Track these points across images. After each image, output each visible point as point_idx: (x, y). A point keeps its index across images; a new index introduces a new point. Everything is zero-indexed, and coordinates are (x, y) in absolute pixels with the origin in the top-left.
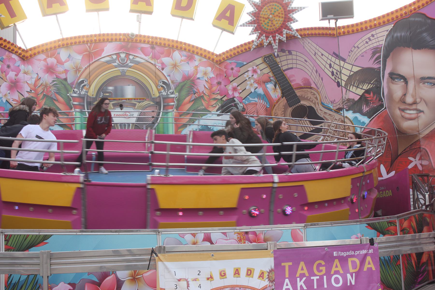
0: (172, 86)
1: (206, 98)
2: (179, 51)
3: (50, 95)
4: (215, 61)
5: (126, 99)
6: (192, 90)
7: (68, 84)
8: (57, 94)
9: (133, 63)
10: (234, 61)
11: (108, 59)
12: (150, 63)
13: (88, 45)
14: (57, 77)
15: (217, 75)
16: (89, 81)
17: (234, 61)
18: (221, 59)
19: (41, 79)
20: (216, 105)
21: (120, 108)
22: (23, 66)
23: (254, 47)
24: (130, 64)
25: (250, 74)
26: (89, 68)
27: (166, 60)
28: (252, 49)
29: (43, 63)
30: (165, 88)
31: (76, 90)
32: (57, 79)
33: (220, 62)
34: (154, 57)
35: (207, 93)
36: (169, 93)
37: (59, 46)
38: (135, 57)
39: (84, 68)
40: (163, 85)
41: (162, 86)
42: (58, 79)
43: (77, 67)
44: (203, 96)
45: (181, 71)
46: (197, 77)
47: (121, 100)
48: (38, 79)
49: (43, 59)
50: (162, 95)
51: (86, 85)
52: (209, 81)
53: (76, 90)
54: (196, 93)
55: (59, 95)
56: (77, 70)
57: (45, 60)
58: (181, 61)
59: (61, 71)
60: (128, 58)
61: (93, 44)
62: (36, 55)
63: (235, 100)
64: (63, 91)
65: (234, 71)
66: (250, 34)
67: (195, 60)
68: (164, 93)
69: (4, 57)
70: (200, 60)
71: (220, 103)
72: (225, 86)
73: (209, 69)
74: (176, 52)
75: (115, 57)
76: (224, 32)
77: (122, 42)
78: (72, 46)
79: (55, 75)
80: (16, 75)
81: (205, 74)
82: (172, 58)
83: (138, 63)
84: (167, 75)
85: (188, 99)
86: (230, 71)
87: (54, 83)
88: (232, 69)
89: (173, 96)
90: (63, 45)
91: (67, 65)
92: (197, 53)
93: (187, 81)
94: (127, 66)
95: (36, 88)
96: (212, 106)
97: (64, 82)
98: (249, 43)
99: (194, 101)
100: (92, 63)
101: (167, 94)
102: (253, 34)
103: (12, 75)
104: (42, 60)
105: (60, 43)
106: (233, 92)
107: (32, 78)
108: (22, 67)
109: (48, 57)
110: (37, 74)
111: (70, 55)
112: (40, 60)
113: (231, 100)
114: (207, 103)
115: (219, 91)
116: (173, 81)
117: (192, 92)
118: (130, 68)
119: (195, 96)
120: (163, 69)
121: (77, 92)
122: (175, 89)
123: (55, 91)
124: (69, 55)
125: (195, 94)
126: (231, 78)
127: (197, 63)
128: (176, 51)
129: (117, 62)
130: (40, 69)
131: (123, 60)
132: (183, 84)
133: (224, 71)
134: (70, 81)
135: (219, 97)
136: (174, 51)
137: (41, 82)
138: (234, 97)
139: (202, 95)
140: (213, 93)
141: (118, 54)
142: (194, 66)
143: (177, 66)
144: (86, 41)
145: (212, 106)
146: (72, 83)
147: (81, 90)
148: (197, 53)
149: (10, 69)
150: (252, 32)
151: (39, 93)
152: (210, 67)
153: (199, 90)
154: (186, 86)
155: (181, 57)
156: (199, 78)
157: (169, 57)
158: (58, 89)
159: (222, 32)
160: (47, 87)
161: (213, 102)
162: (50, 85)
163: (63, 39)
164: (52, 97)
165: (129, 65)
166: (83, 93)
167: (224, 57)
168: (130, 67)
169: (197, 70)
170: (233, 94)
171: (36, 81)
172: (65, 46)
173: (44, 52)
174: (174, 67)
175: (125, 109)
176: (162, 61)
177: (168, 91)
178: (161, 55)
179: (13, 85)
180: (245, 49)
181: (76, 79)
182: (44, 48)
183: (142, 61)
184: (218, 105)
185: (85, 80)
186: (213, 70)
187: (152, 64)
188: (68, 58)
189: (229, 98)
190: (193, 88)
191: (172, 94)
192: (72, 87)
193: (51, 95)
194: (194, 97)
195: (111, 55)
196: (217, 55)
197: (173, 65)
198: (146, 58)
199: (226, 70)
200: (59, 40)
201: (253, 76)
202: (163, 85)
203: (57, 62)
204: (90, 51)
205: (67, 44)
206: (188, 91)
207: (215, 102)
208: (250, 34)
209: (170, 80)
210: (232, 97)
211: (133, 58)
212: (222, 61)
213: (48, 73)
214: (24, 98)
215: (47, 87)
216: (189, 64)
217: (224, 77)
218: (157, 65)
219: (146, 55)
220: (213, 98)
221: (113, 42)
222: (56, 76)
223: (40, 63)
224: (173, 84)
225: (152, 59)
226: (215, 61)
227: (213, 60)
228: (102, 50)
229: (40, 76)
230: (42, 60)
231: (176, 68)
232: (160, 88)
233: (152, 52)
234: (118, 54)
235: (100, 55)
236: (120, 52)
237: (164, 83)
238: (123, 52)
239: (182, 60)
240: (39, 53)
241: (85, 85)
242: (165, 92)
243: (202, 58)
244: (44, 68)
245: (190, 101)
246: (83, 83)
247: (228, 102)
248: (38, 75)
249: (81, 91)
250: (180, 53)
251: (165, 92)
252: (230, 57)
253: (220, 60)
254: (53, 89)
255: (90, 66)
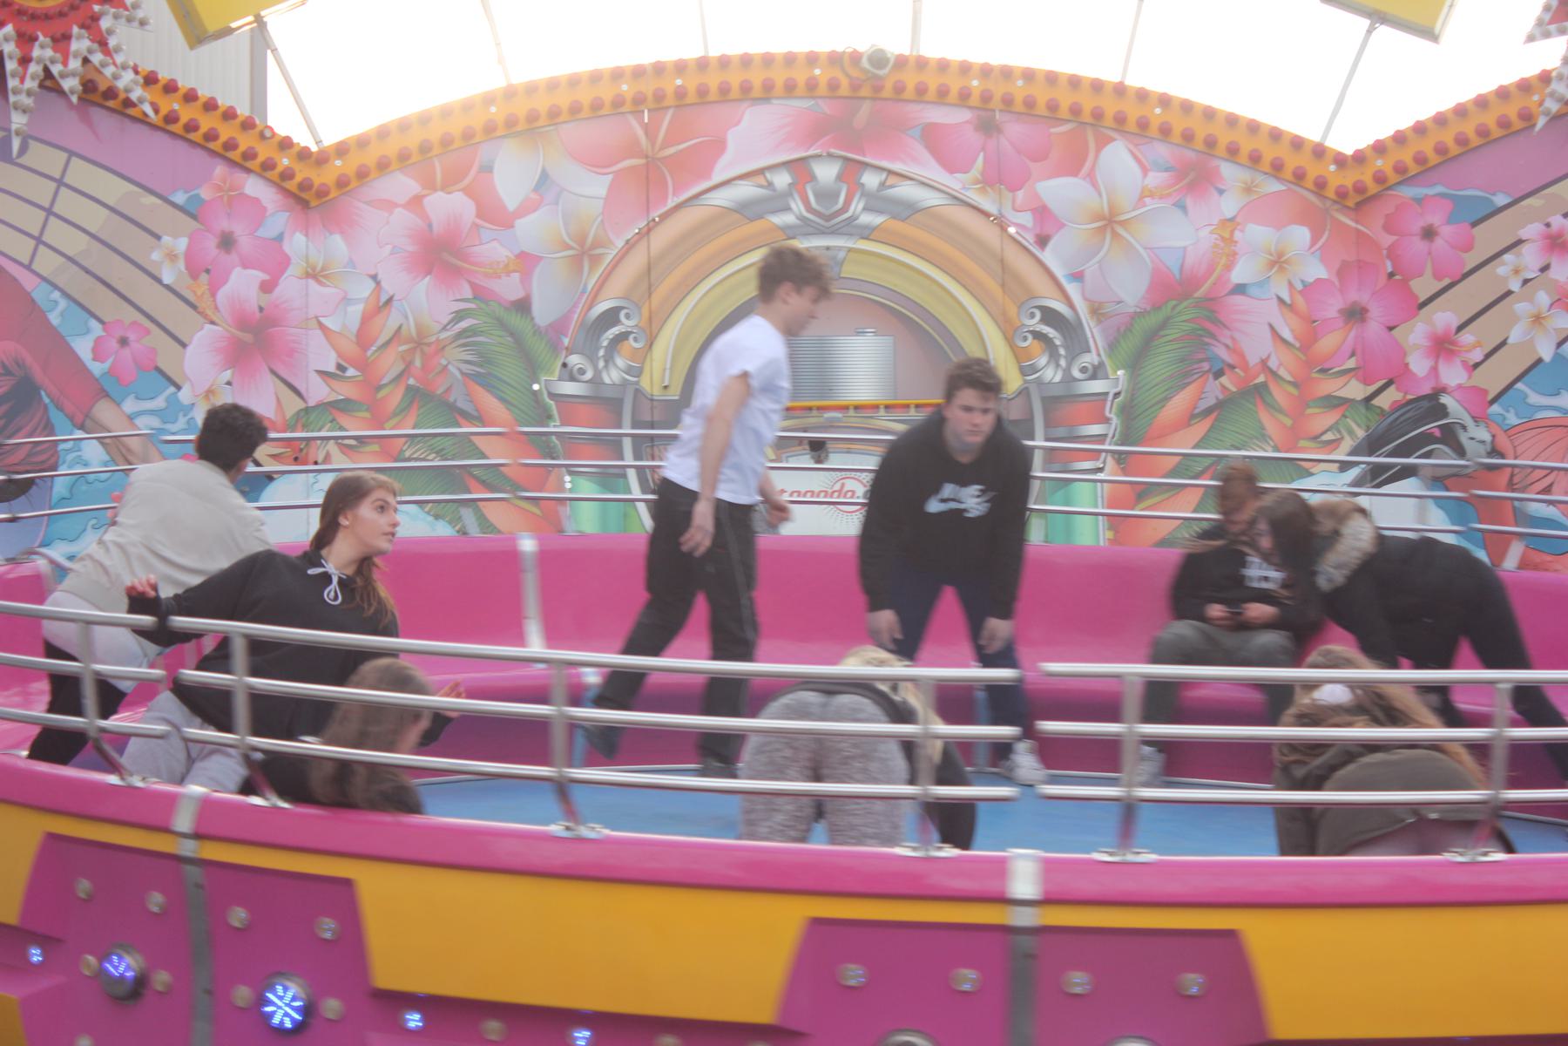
0: (1094, 333)
1: (1279, 395)
2: (1136, 145)
3: (439, 392)
4: (1330, 192)
5: (844, 408)
6: (1201, 356)
7: (537, 331)
8: (480, 385)
9: (881, 212)
10: (1439, 189)
11: (745, 191)
12: (971, 209)
13: (641, 121)
14: (480, 294)
15: (1343, 272)
16: (645, 311)
17: (1439, 189)
18: (1367, 178)
19: (395, 303)
20: (1339, 432)
21: (813, 457)
22: (299, 238)
23: (1553, 106)
24: (867, 219)
25: (1530, 257)
26: (644, 243)
27: (1058, 190)
28: (1541, 122)
29: (402, 219)
30: (1058, 342)
31: (575, 360)
32: (478, 302)
33: (1358, 200)
34: (995, 178)
35: (1290, 372)
36: (1076, 373)
37: (490, 129)
38: (890, 181)
39: (620, 244)
40: (1046, 329)
41: (1038, 336)
42: (483, 306)
43: (582, 242)
44: (1264, 385)
45: (1145, 248)
46: (1229, 280)
47: (815, 413)
48: (380, 308)
49: (402, 200)
50: (1039, 382)
51: (631, 332)
52: (1300, 302)
53: (575, 360)
54: (1227, 370)
55: (488, 391)
56: (583, 252)
57: (415, 203)
58: (1141, 198)
59: (498, 262)
60: (855, 187)
61: (670, 113)
62: (368, 179)
63: (1444, 407)
64: (510, 370)
65: (1439, 243)
66: (1531, 38)
67: (1223, 187)
68: (1052, 375)
69: (205, 193)
70: (1248, 190)
71: (1359, 425)
72: (1391, 329)
73: (1300, 235)
74: (1115, 143)
75: (782, 180)
76: (1383, 31)
77: (820, 102)
78: (557, 124)
79: (470, 282)
80: (267, 287)
81: (1278, 262)
82: (1091, 178)
83: (908, 211)
84: (1064, 276)
85: (1180, 402)
86: (1419, 245)
87: (464, 324)
88: (1429, 233)
89: (1097, 386)
90: (511, 122)
91: (533, 231)
92: (1233, 151)
93: (1174, 303)
94: (850, 228)
95: (369, 353)
96: (1315, 438)
97: (515, 320)
98: (1524, 86)
99: (1215, 414)
100: (664, 217)
101: (1069, 379)
102: (1547, 35)
103: (242, 284)
104: (395, 205)
105: (493, 109)
106: (1433, 363)
107: (346, 300)
108: (297, 244)
109: (430, 185)
110: (374, 277)
111: (544, 176)
112: (390, 205)
113: (1425, 404)
114: (1288, 422)
115: (1353, 354)
116: (1101, 303)
117: (1206, 366)
118: (863, 238)
119: (1223, 387)
120: (1043, 241)
121: (582, 372)
122: (1112, 347)
123: (465, 368)
124: (540, 178)
125: (1218, 374)
126: (1423, 286)
127: (1229, 205)
128: (1111, 140)
129: (797, 205)
130: (391, 254)
131: (827, 195)
132: (1154, 320)
133: (1386, 246)
134: (544, 312)
135: (1355, 390)
136: (1103, 142)
137: (392, 321)
138: (1442, 390)
139: (1261, 379)
140: (1324, 371)
141: (800, 168)
142: (1215, 222)
143: (1122, 223)
144: (629, 97)
145: (1315, 438)
146: (559, 327)
147: (601, 364)
148: (1233, 151)
149: (234, 257)
150: (1540, 23)
151: (384, 381)
152: (1302, 223)
153: (1242, 356)
154: (1173, 333)
155: (1145, 171)
156: (1240, 289)
157: (1073, 171)
158: (485, 359)
159: (1369, 32)
160: (426, 349)
161: (1323, 420)
162: (443, 335)
163: (510, 93)
164: (452, 399)
165: (856, 222)
166: (612, 376)
167: (1379, 171)
168: (867, 233)
169: (1230, 241)
170: (1434, 370)
171: (366, 319)
172: (520, 128)
173: (414, 159)
174: (1105, 227)
175: (835, 461)
176: (1037, 196)
177: (1071, 359)
178: (1031, 165)
179: (247, 337)
180: (1504, 123)
181: (575, 305)
182: (412, 141)
183: (930, 199)
184: (1351, 433)
185: (622, 308)
186: (1320, 243)
187: (987, 214)
188: (536, 189)
189: (1410, 397)
190: (1208, 344)
191: (1094, 377)
192: (555, 347)
193: (448, 390)
194: (1213, 391)
195: (760, 172)
196: (1340, 160)
197: (1098, 217)
198: (953, 182)
199: (1395, 238)
200: (489, 99)
201: (1545, 269)
202: (1046, 329)
203: (479, 216)
204: (650, 154)
205: (532, 117)
206: (1182, 360)
207: (1330, 418)
208: (1531, 38)
209: (1085, 299)
210: (1426, 389)
211: (883, 185)
212: (1373, 188)
213: (429, 272)
214: (301, 405)
215: (426, 349)
216: (1184, 208)
217: (1382, 280)
218: (1015, 221)
219: (951, 167)
220: (1326, 393)
221: (775, 101)
222: (474, 287)
223: (388, 223)
224: (1099, 322)
225: (982, 190)
226: (1330, 192)
227: (1321, 184)
228: (719, 146)
229: (388, 288)
230: (395, 205)
231: (1115, 235)
232: (1025, 344)
233: (983, 149)
234: (800, 168)
235: (706, 172)
236: (811, 152)
237: (1050, 316)
238: (830, 156)
239: (1151, 191)
240: (383, 166)
241: (623, 337)
242: (1058, 365)
243: (1260, 178)
244: (411, 248)
245: (1193, 416)
246: (617, 322)
247: (1402, 419)
248: (378, 283)
249: (606, 366)
250: (1134, 150)
251: (1058, 365)
252: (1414, 169)
253: (1359, 188)
254: (455, 360)
255: (649, 230)
